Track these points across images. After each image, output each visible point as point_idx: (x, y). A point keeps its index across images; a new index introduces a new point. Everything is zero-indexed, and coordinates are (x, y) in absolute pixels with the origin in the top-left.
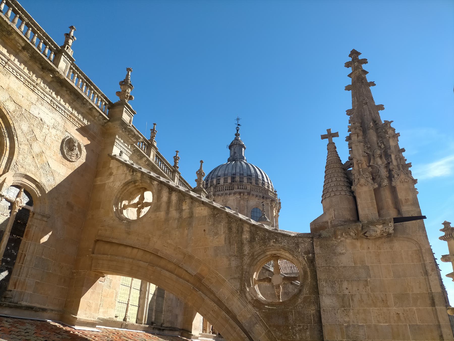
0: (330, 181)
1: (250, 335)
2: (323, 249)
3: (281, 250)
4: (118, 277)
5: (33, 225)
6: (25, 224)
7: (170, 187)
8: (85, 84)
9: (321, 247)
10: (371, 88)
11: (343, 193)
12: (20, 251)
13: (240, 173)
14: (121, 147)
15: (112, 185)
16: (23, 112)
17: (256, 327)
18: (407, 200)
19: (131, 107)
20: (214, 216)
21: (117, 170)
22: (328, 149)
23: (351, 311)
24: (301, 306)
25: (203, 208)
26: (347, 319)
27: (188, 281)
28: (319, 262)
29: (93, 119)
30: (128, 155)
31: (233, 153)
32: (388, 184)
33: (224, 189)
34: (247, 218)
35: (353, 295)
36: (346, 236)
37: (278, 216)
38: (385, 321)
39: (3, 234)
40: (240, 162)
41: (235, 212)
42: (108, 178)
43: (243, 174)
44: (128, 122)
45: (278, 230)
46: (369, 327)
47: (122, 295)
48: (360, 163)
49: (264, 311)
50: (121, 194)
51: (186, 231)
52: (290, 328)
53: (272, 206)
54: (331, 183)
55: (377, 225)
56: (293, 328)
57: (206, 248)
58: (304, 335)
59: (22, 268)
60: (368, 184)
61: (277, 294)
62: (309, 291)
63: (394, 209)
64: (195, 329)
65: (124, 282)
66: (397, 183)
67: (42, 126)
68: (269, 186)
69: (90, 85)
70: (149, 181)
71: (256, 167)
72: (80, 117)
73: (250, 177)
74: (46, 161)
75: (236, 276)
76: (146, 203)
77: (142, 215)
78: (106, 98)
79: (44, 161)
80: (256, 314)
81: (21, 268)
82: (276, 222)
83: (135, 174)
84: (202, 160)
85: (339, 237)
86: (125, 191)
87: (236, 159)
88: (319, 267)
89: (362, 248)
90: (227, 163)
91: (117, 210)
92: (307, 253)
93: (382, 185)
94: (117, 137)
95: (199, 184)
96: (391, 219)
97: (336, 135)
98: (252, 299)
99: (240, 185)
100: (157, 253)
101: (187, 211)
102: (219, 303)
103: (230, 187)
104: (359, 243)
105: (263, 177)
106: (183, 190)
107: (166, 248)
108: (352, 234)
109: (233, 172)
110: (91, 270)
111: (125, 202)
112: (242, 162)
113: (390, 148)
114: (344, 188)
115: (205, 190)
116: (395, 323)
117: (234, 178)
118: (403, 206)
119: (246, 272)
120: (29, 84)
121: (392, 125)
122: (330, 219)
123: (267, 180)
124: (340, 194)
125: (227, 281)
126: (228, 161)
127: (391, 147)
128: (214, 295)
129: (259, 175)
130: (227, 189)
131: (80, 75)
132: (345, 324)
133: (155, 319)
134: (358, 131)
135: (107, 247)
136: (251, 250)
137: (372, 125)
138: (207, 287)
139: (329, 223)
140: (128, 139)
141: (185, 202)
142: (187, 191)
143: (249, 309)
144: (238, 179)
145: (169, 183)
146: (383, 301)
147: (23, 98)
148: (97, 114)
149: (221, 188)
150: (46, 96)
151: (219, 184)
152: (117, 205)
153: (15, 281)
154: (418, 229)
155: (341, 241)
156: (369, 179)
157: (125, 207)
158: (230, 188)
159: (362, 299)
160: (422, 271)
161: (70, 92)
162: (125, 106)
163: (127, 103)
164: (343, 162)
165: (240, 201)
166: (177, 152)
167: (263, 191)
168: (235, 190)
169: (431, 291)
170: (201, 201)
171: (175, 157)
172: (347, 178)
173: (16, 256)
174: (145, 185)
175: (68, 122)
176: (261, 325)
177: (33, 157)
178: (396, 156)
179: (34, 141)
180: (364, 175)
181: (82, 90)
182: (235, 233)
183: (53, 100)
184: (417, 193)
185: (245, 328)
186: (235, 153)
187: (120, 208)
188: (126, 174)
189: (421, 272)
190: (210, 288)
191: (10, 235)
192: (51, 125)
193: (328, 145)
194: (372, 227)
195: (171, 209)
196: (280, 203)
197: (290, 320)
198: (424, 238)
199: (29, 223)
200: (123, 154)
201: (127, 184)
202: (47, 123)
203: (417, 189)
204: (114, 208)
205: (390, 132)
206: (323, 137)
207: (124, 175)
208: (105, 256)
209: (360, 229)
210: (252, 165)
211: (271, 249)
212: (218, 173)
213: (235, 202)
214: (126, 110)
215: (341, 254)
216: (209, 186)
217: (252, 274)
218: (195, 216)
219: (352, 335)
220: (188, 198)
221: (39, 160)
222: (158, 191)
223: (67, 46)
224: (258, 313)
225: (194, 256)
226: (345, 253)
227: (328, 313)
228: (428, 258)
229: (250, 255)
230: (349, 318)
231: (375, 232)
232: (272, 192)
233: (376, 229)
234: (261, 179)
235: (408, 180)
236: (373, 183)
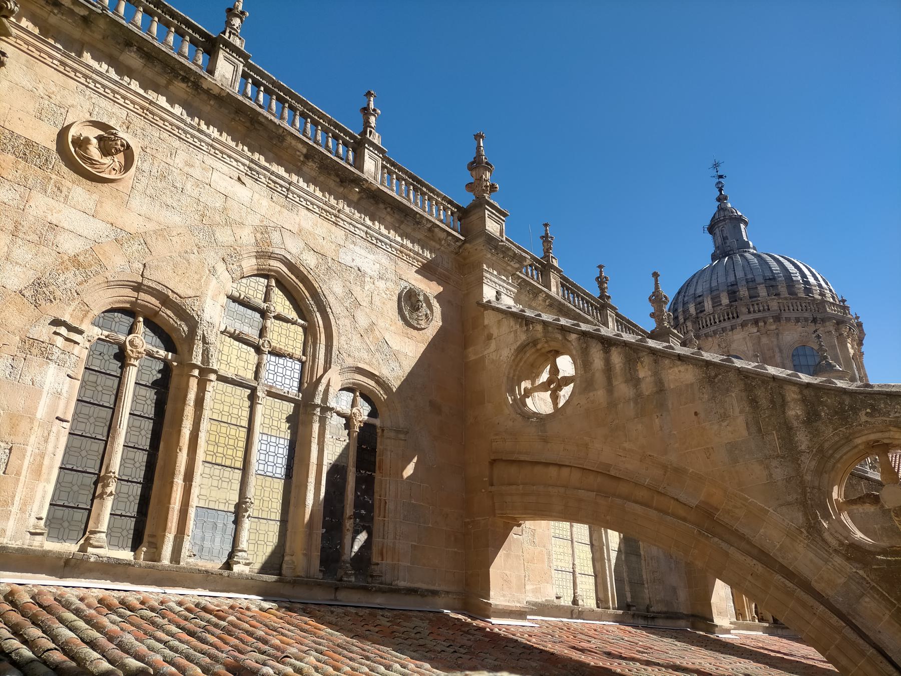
1: (854, 621)
4: (544, 523)
6: (374, 450)
7: (603, 338)
8: (412, 188)
12: (376, 496)
13: (746, 279)
14: (496, 283)
15: (496, 357)
16: (329, 265)
19: (497, 205)
20: (711, 381)
21: (499, 328)
25: (682, 368)
27: (684, 519)
29: (438, 246)
30: (512, 296)
31: (719, 240)
33: (717, 321)
34: (790, 372)
37: (862, 354)
39: (346, 472)
41: (757, 364)
42: (487, 345)
43: (753, 280)
44: (498, 234)
45: (872, 386)
47: (559, 557)
49: (875, 567)
50: (515, 371)
51: (657, 420)
53: (841, 334)
57: (708, 448)
59: (386, 524)
64: (720, 613)
65: (557, 531)
67: (363, 279)
68: (824, 291)
69: (419, 186)
71: (782, 257)
72: (417, 248)
73: (773, 283)
74: (381, 339)
75: (790, 499)
76: (564, 378)
77: (561, 403)
78: (450, 202)
79: (378, 339)
80: (857, 576)
81: (384, 525)
82: (859, 370)
83: (531, 328)
87: (730, 251)
90: (711, 264)
91: (514, 400)
94: (485, 267)
95: (660, 321)
99: (753, 305)
100: (609, 471)
101: (649, 380)
102: (763, 557)
103: (730, 314)
105: (803, 275)
106: (631, 340)
107: (624, 459)
109: (729, 281)
110: (495, 516)
111: (526, 384)
112: (747, 255)
115: (676, 331)
117: (735, 292)
119: (814, 488)
120: (328, 214)
123: (816, 279)
125: (772, 511)
126: (713, 259)
128: (749, 542)
129: (793, 273)
130: (724, 320)
131: (400, 173)
136: (815, 440)
138: (728, 526)
140: (505, 265)
141: (642, 363)
142: (640, 340)
143: (838, 565)
144: (743, 292)
145: (600, 331)
149: (710, 320)
150: (357, 228)
151: (701, 312)
152: (512, 392)
153: (380, 548)
157: (528, 393)
158: (731, 316)
161: (392, 209)
162: (486, 206)
163: (489, 200)
165: (759, 338)
166: (600, 267)
167: (812, 307)
168: (743, 318)
170: (674, 356)
171: (598, 278)
173: (373, 505)
174: (554, 345)
175: (399, 262)
176: (875, 598)
177: (361, 336)
181: (409, 200)
182: (767, 409)
183: (369, 231)
185: (838, 606)
186: (725, 239)
187: (519, 397)
188: (516, 332)
190: (736, 530)
191: (357, 471)
192: (375, 274)
195: (615, 383)
196: (860, 325)
199: (379, 447)
200: (502, 296)
201: (522, 349)
204: (509, 398)
207: (512, 335)
208: (514, 487)
210: (771, 256)
211: (863, 430)
212: (695, 290)
213: (748, 344)
214: (490, 214)
216: (682, 321)
217: (828, 490)
220: (645, 353)
221: (371, 339)
222: (582, 353)
223: (368, 131)
225: (685, 468)
229: (814, 450)
232: (834, 304)
234: (801, 281)
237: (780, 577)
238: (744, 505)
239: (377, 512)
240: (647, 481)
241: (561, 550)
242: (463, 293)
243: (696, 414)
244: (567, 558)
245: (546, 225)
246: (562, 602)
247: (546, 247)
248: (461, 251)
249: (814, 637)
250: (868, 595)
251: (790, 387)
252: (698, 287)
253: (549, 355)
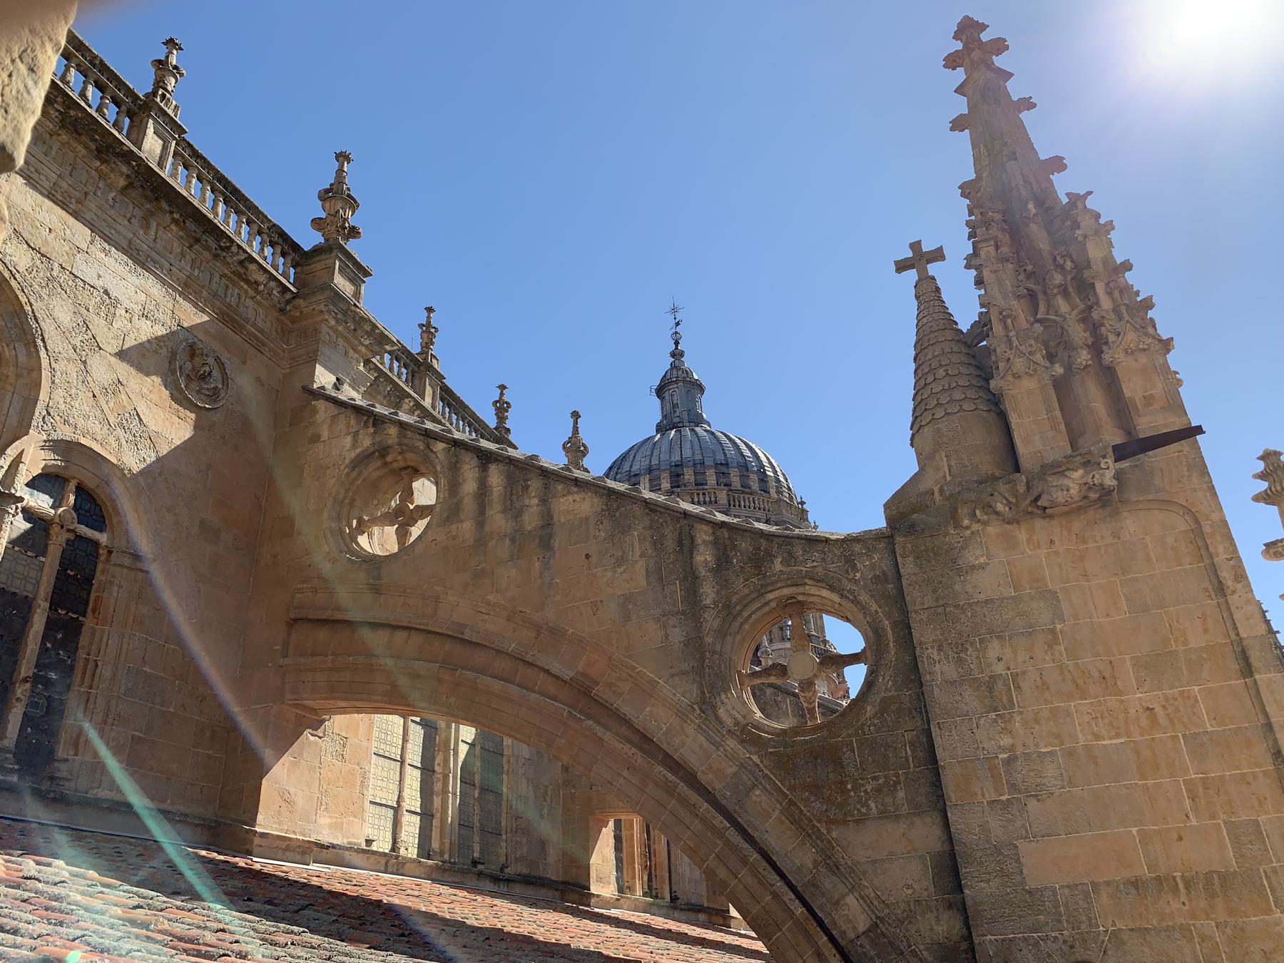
0: (930, 379)
1: (739, 820)
2: (924, 562)
3: (806, 584)
5: (111, 583)
6: (89, 580)
9: (918, 558)
10: (1025, 116)
11: (968, 406)
12: (82, 654)
16: (55, 274)
17: (755, 798)
18: (1149, 400)
22: (917, 297)
23: (1018, 718)
24: (875, 725)
25: (577, 497)
26: (1006, 741)
27: (554, 699)
28: (918, 599)
31: (668, 407)
32: (1090, 362)
35: (1017, 675)
36: (985, 517)
38: (1113, 733)
39: (30, 607)
40: (693, 430)
46: (1071, 754)
48: (1008, 316)
50: (347, 491)
51: (537, 564)
52: (849, 787)
54: (933, 385)
55: (1068, 469)
56: (854, 789)
57: (596, 602)
58: (889, 800)
59: (92, 699)
60: (1035, 370)
61: (805, 705)
62: (895, 682)
63: (1116, 430)
64: (600, 880)
66: (1117, 356)
67: (112, 310)
70: (421, 446)
71: (740, 439)
73: (724, 469)
74: (129, 408)
75: (685, 666)
79: (125, 407)
84: (575, 412)
85: (966, 522)
86: (359, 482)
88: (916, 612)
89: (1034, 544)
92: (881, 579)
93: (1074, 366)
96: (1105, 447)
97: (938, 255)
98: (737, 723)
99: (698, 494)
100: (463, 634)
102: (645, 741)
104: (1023, 532)
107: (486, 617)
108: (1000, 507)
109: (673, 459)
110: (283, 703)
112: (698, 429)
113: (1089, 266)
114: (971, 393)
116: (1142, 735)
117: (678, 475)
118: (1139, 416)
119: (714, 652)
121: (1090, 203)
122: (936, 482)
124: (961, 409)
125: (662, 683)
127: (1093, 261)
132: (1001, 756)
133: (481, 852)
134: (994, 231)
135: (322, 634)
137: (1034, 210)
138: (607, 705)
139: (936, 494)
143: (731, 751)
144: (689, 475)
146: (1104, 678)
147: (53, 235)
148: (262, 278)
150: (115, 229)
154: (1186, 473)
155: (973, 533)
156: (1038, 357)
159: (1044, 683)
160: (1207, 585)
161: (181, 215)
164: (964, 326)
169: (1238, 635)
171: (496, 402)
172: (977, 367)
174: (412, 458)
176: (767, 790)
177: (94, 396)
178: (1109, 282)
179: (93, 351)
180: (1022, 348)
184: (1179, 382)
185: (724, 802)
186: (675, 406)
188: (357, 433)
189: (1206, 590)
191: (50, 608)
192: (137, 308)
193: (915, 287)
194: (1054, 481)
195: (489, 512)
197: (848, 765)
198: (1208, 494)
199: (99, 577)
201: (362, 460)
202: (126, 303)
203: (1178, 373)
205: (1086, 223)
206: (902, 266)
208: (318, 659)
209: (1022, 489)
211: (776, 582)
212: (631, 466)
215: (973, 567)
217: (730, 658)
218: (559, 521)
219: (1024, 781)
221: (111, 405)
223: (160, 93)
224: (755, 758)
226: (988, 564)
227: (953, 732)
228: (1221, 549)
229: (720, 605)
230: (1013, 737)
231: (1065, 492)
233: (1066, 482)
235: (1148, 345)
236: (1048, 364)
237: (662, 769)
238: (630, 676)
239: (79, 679)
240: (513, 646)
241: (385, 774)
242: (283, 371)
243: (587, 556)
244: (391, 786)
245: (430, 310)
246: (374, 847)
247: (426, 340)
248: (288, 308)
249: (692, 846)
250: (760, 787)
251: (703, 526)
252: (635, 463)
253: (403, 473)
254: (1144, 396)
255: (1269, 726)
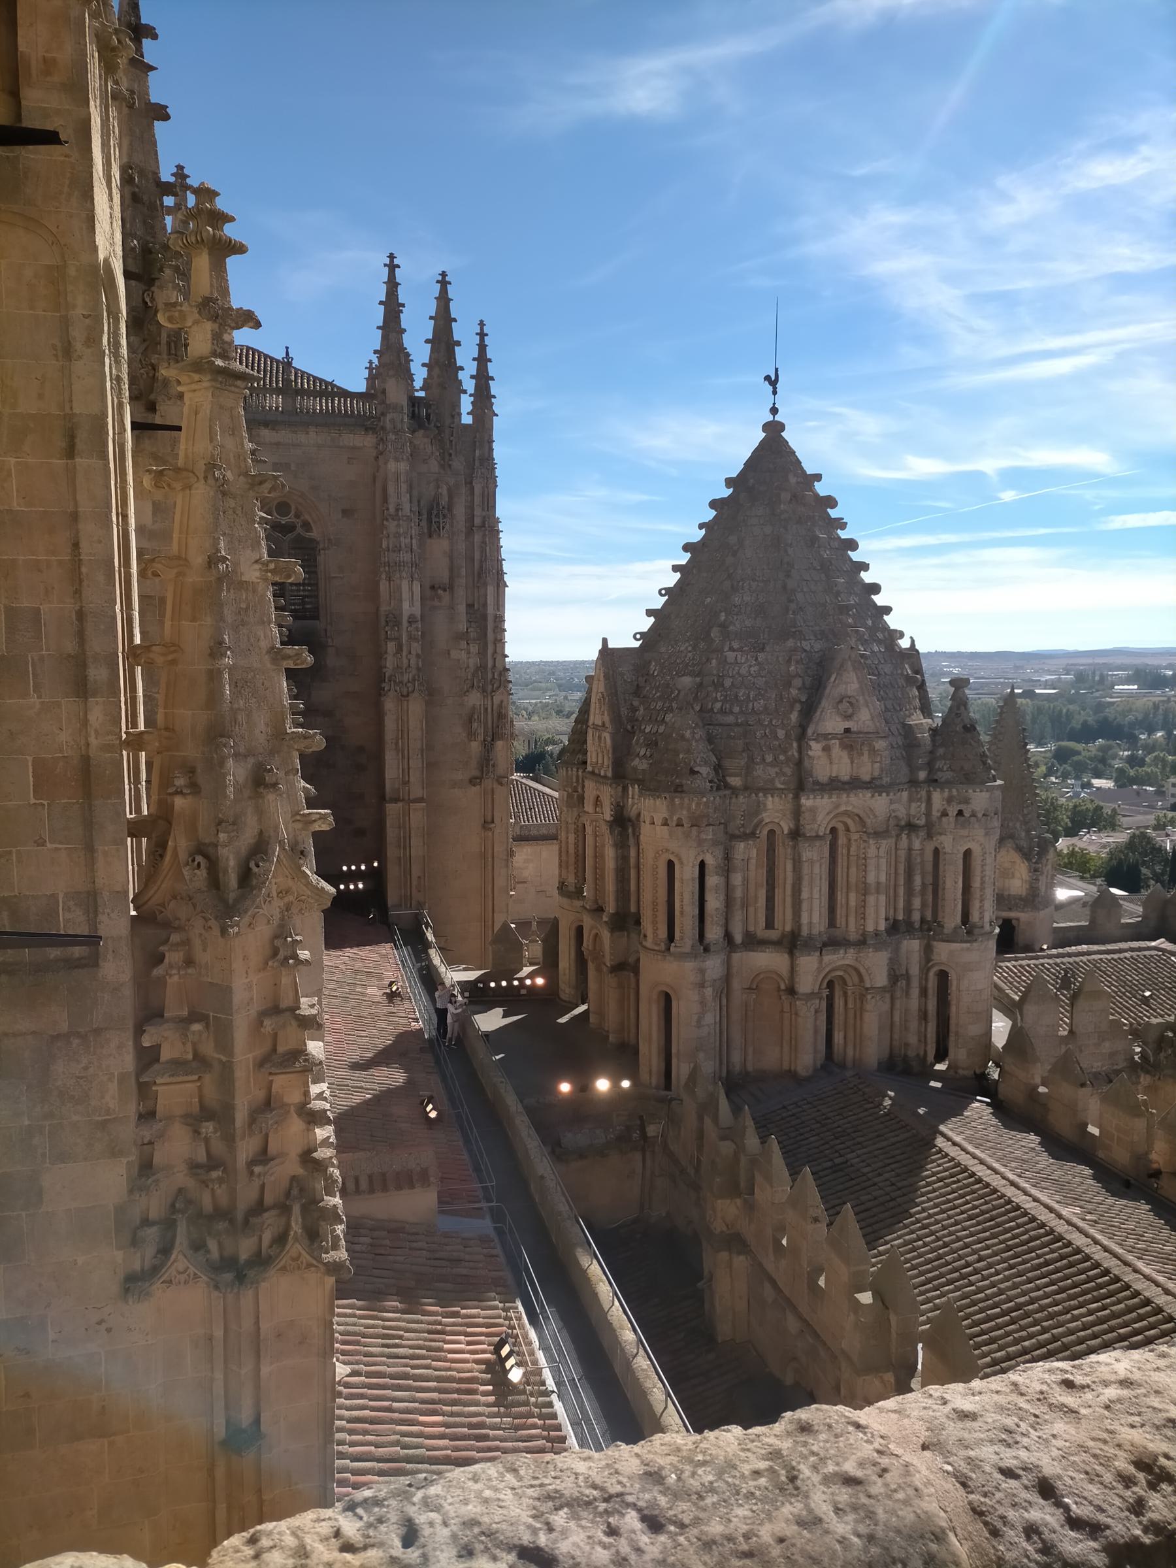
18: (49, 65)
169: (71, 408)
189: (54, 347)
254: (44, 59)
255: (75, 517)
